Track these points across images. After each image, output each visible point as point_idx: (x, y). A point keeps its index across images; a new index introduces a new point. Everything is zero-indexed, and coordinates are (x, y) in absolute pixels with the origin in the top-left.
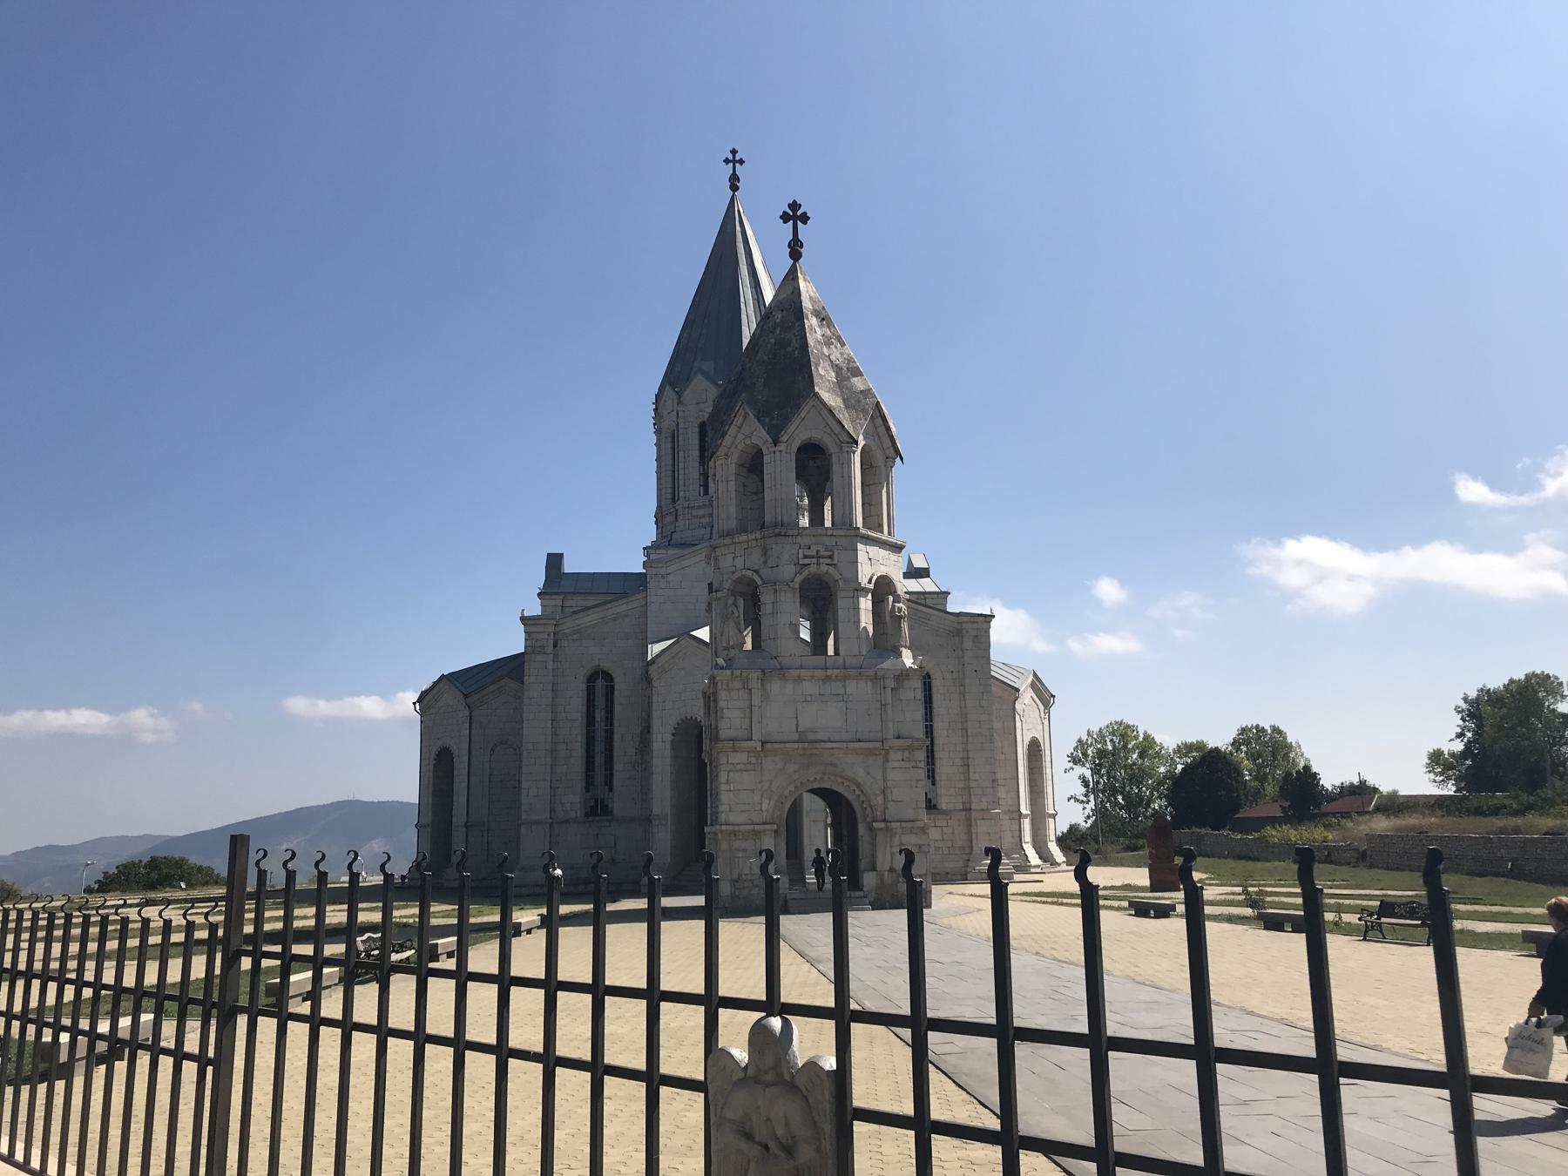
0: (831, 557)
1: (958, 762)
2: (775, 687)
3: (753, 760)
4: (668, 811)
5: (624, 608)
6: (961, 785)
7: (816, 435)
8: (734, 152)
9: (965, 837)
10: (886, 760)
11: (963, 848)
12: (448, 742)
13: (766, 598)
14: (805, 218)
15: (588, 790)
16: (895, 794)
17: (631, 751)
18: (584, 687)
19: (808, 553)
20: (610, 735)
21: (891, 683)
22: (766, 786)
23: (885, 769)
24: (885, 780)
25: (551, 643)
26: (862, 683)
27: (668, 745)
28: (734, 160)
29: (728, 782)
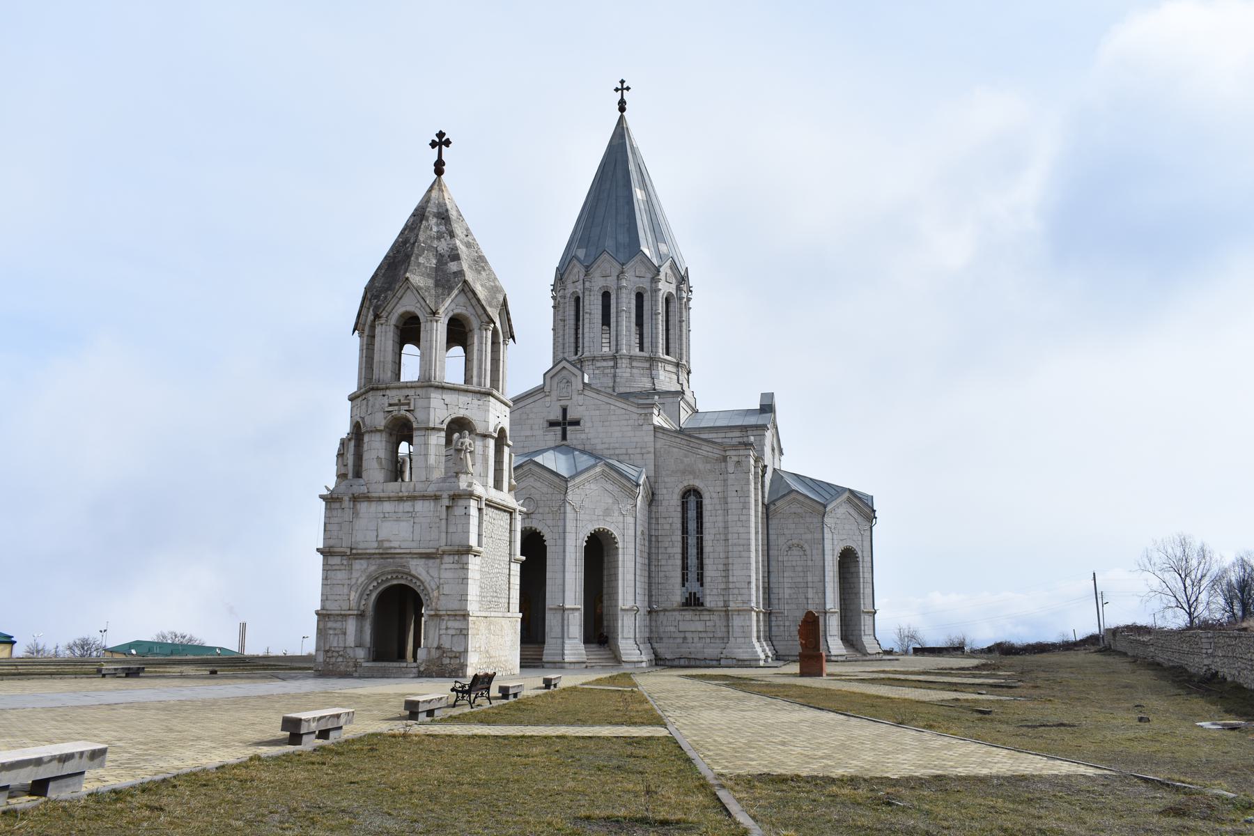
0: (409, 404)
1: (721, 567)
2: (363, 507)
6: (723, 586)
7: (411, 308)
8: (622, 82)
9: (724, 629)
11: (723, 638)
13: (366, 438)
14: (448, 143)
16: (446, 589)
19: (392, 402)
21: (446, 502)
22: (354, 581)
23: (440, 569)
26: (427, 503)
28: (623, 88)
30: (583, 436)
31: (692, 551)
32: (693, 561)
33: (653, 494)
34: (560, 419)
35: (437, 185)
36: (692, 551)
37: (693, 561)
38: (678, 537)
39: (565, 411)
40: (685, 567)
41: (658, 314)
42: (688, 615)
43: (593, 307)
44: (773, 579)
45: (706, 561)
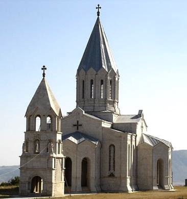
8: (99, 5)
28: (99, 8)
30: (82, 129)
31: (112, 161)
32: (112, 164)
33: (101, 146)
34: (76, 124)
36: (112, 161)
37: (112, 164)
38: (108, 158)
39: (78, 122)
40: (110, 166)
41: (110, 81)
42: (111, 179)
43: (88, 83)
44: (138, 167)
45: (115, 164)
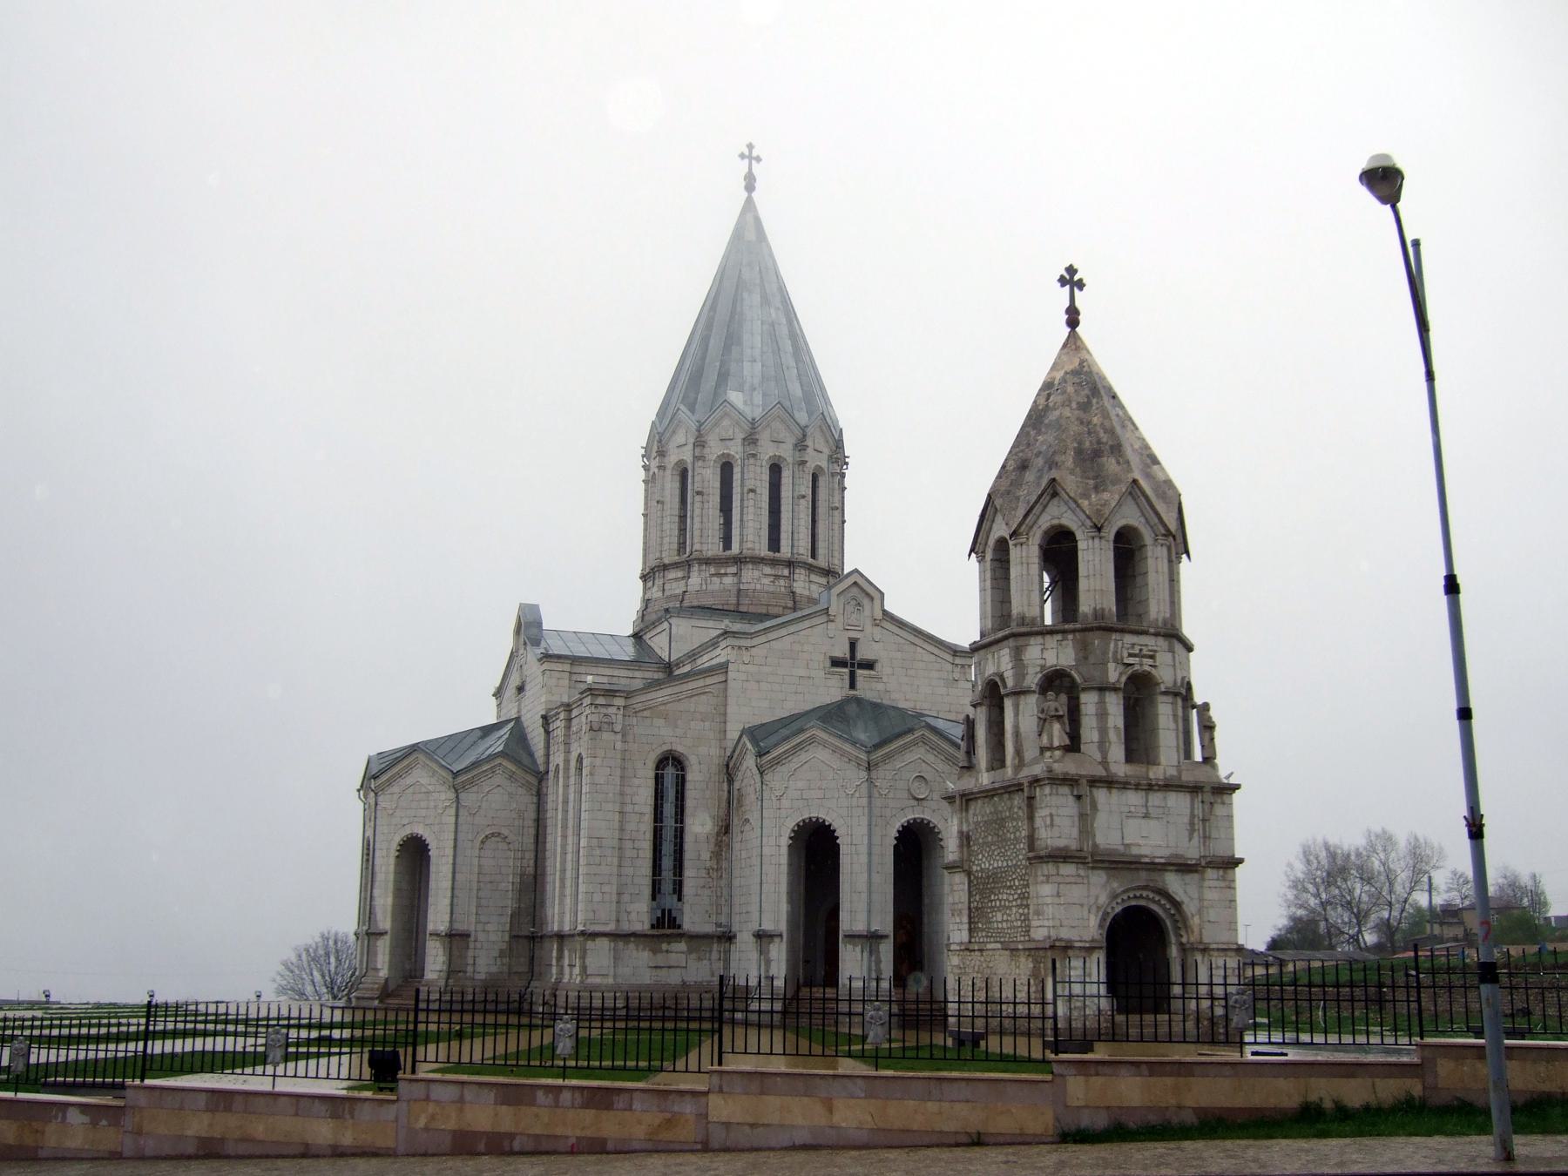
2: (1101, 795)
3: (1082, 872)
4: (783, 927)
5: (701, 683)
8: (750, 147)
10: (1203, 879)
12: (420, 830)
14: (1080, 285)
15: (654, 898)
16: (1212, 915)
17: (706, 855)
18: (652, 774)
20: (680, 834)
22: (1092, 901)
24: (1201, 900)
25: (620, 717)
27: (784, 850)
28: (750, 156)
29: (1058, 895)
35: (1073, 343)
39: (853, 645)
